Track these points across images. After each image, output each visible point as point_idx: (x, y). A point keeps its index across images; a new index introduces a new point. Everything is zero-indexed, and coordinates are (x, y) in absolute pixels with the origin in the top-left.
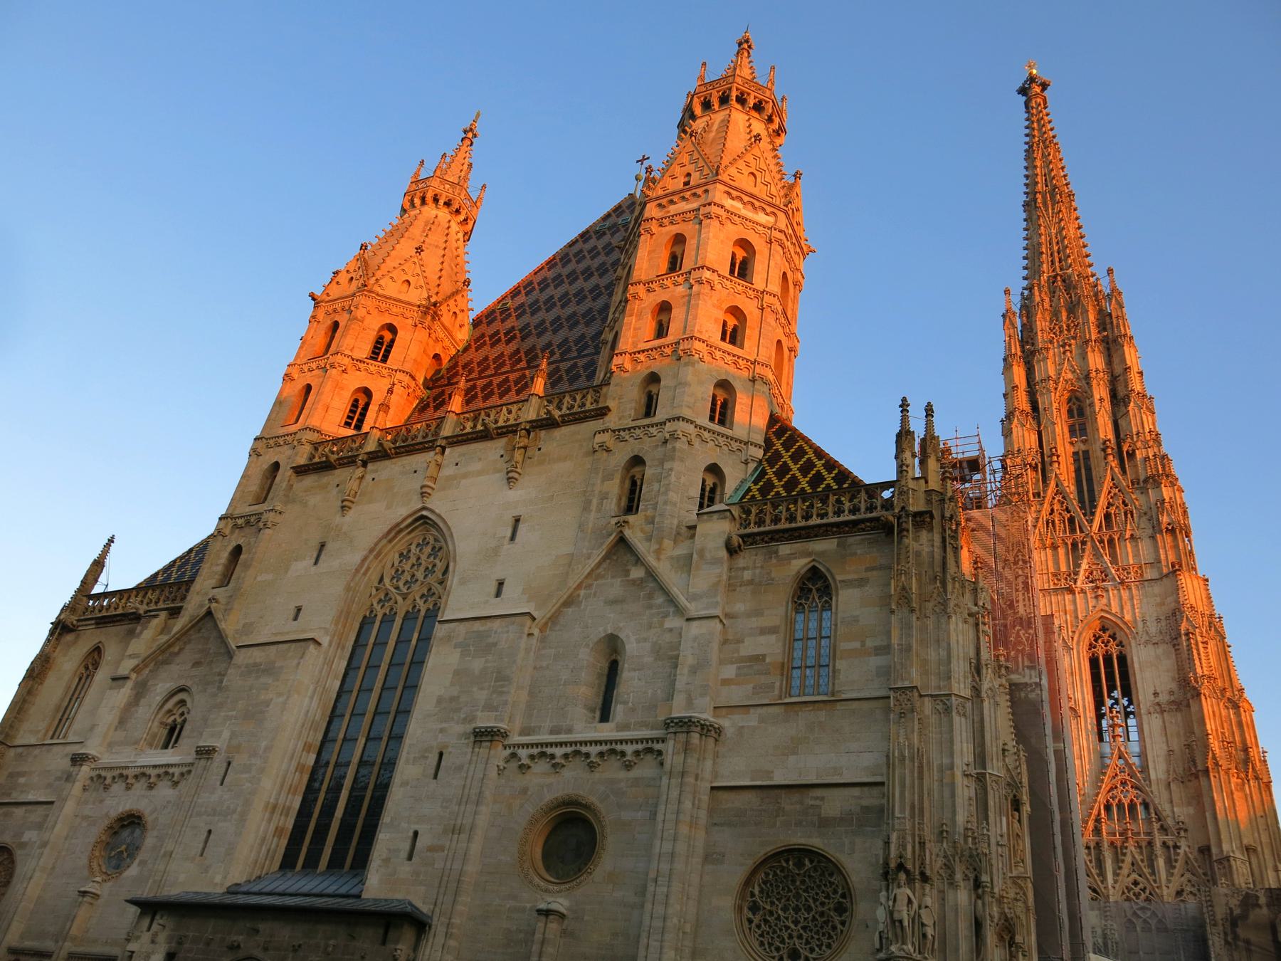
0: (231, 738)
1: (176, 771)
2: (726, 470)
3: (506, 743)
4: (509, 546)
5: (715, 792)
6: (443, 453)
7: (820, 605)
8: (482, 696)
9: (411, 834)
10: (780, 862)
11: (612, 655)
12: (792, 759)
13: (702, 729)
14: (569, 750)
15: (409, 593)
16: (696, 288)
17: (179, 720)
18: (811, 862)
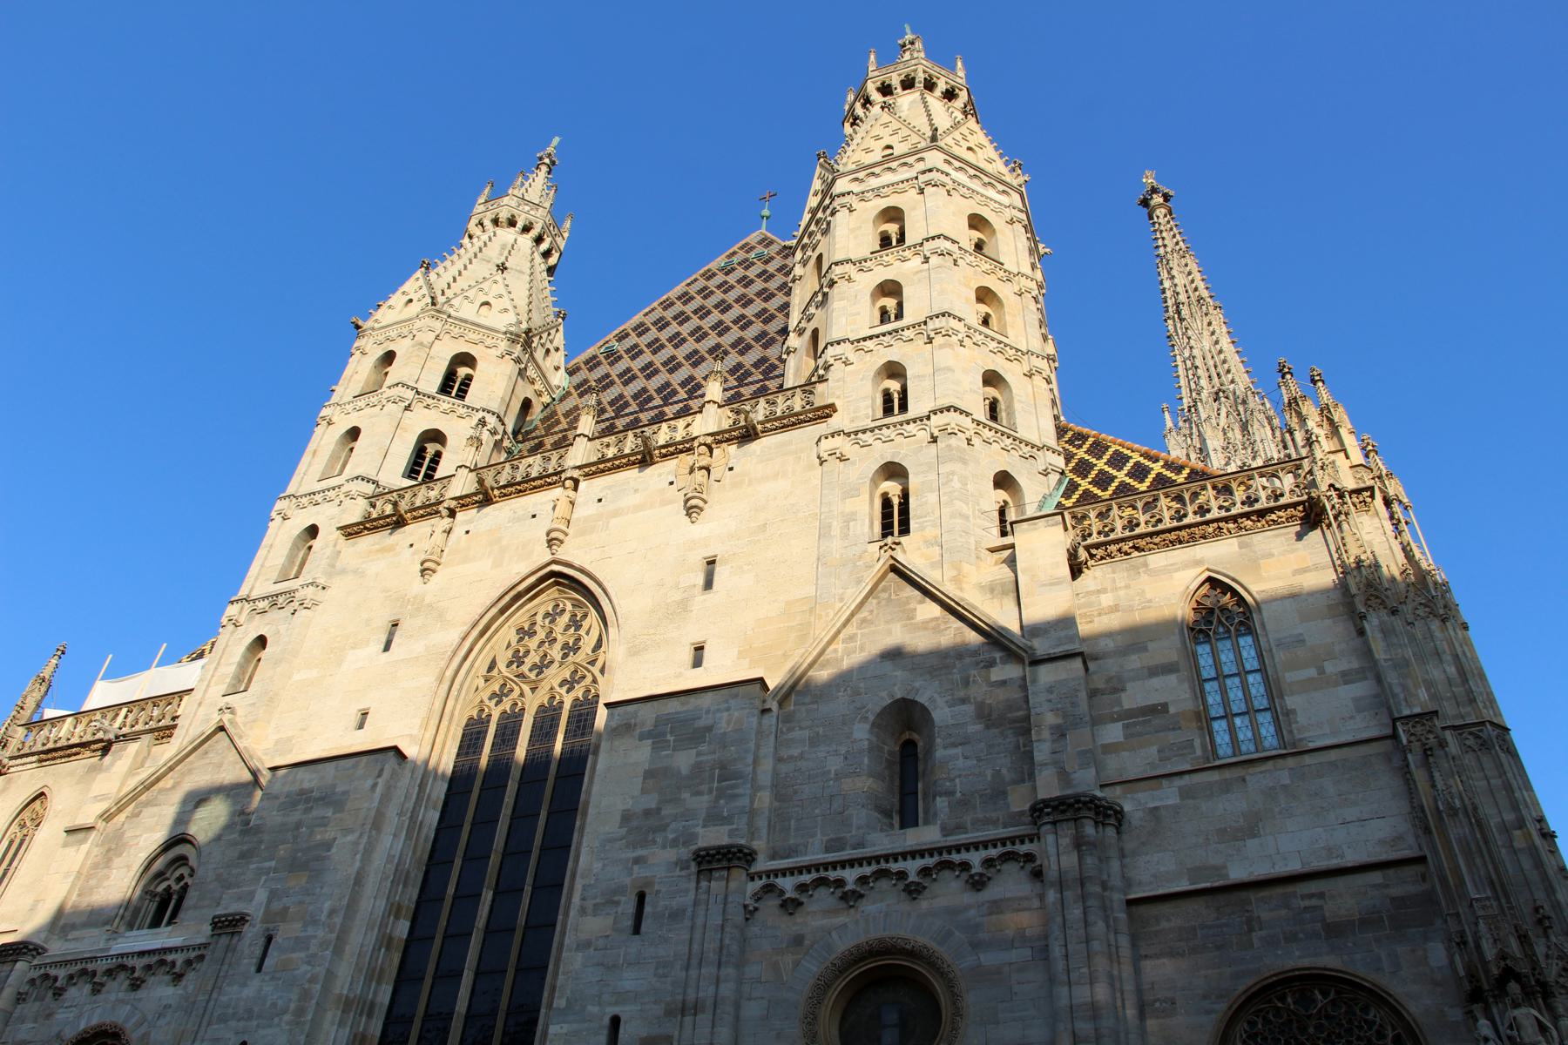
0: (270, 901)
1: (179, 958)
2: (1022, 479)
3: (752, 870)
5: (1134, 909)
6: (576, 489)
7: (1232, 629)
8: (701, 803)
9: (606, 1021)
10: (1270, 1001)
11: (901, 734)
12: (1252, 844)
13: (1097, 814)
14: (867, 870)
15: (542, 680)
16: (934, 260)
17: (175, 887)
18: (1325, 994)
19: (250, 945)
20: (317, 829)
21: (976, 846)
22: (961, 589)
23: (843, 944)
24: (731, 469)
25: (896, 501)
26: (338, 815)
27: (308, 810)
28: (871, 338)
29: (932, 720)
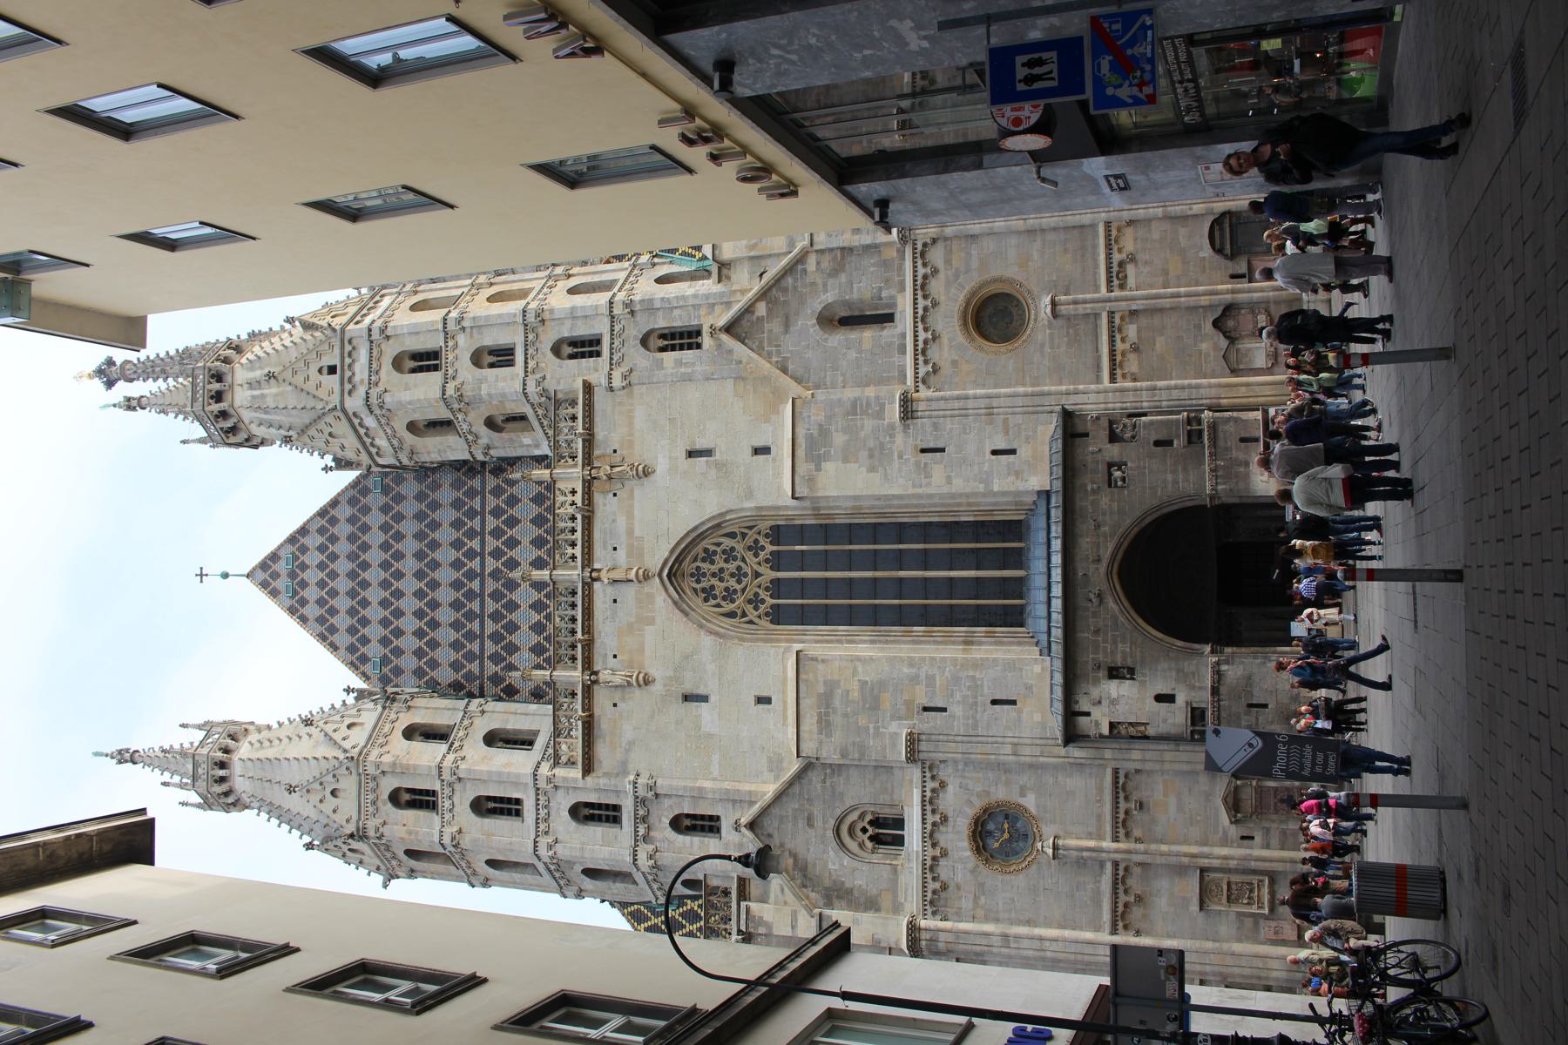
0: (900, 718)
1: (930, 785)
4: (717, 454)
6: (599, 570)
14: (921, 326)
16: (466, 324)
17: (871, 831)
19: (928, 722)
20: (850, 698)
22: (751, 289)
23: (961, 338)
24: (615, 451)
25: (666, 343)
26: (842, 684)
27: (835, 711)
28: (526, 363)
29: (834, 302)
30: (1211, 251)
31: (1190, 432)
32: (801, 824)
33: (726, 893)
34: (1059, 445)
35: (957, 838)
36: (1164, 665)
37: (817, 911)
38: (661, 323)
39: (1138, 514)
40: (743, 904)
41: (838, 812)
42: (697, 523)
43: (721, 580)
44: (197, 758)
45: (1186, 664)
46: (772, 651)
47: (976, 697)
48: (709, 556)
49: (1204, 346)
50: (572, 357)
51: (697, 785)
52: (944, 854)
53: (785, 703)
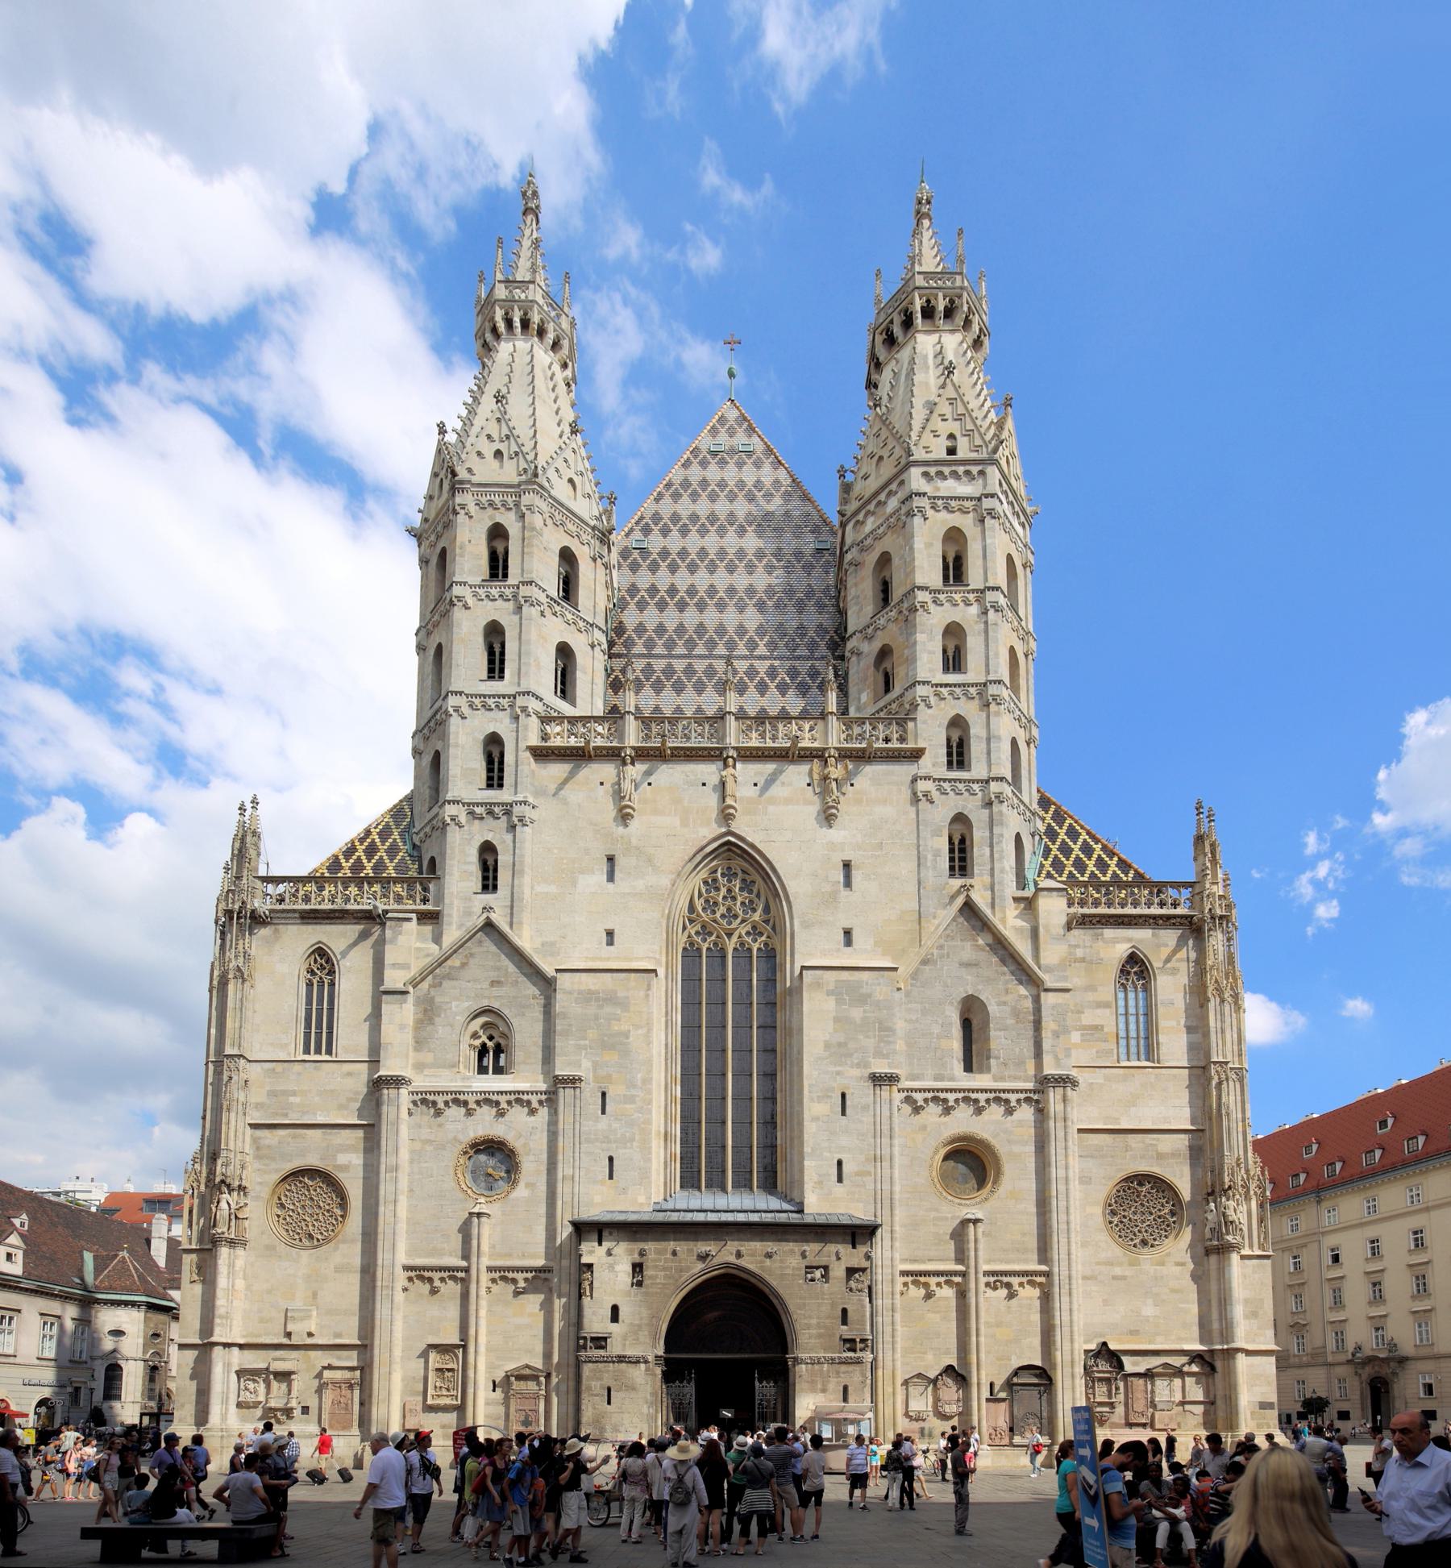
0: (595, 1070)
20: (613, 1022)
21: (1013, 1091)
30: (1017, 1366)
31: (853, 1341)
32: (493, 975)
33: (425, 900)
34: (845, 1221)
35: (484, 1124)
36: (645, 1313)
37: (411, 989)
38: (979, 835)
39: (781, 1291)
40: (414, 916)
41: (506, 1011)
42: (779, 871)
43: (725, 898)
44: (531, 286)
45: (646, 1333)
46: (656, 947)
47: (615, 1142)
48: (747, 886)
49: (930, 1357)
50: (949, 740)
51: (526, 869)
52: (469, 1113)
53: (608, 959)
